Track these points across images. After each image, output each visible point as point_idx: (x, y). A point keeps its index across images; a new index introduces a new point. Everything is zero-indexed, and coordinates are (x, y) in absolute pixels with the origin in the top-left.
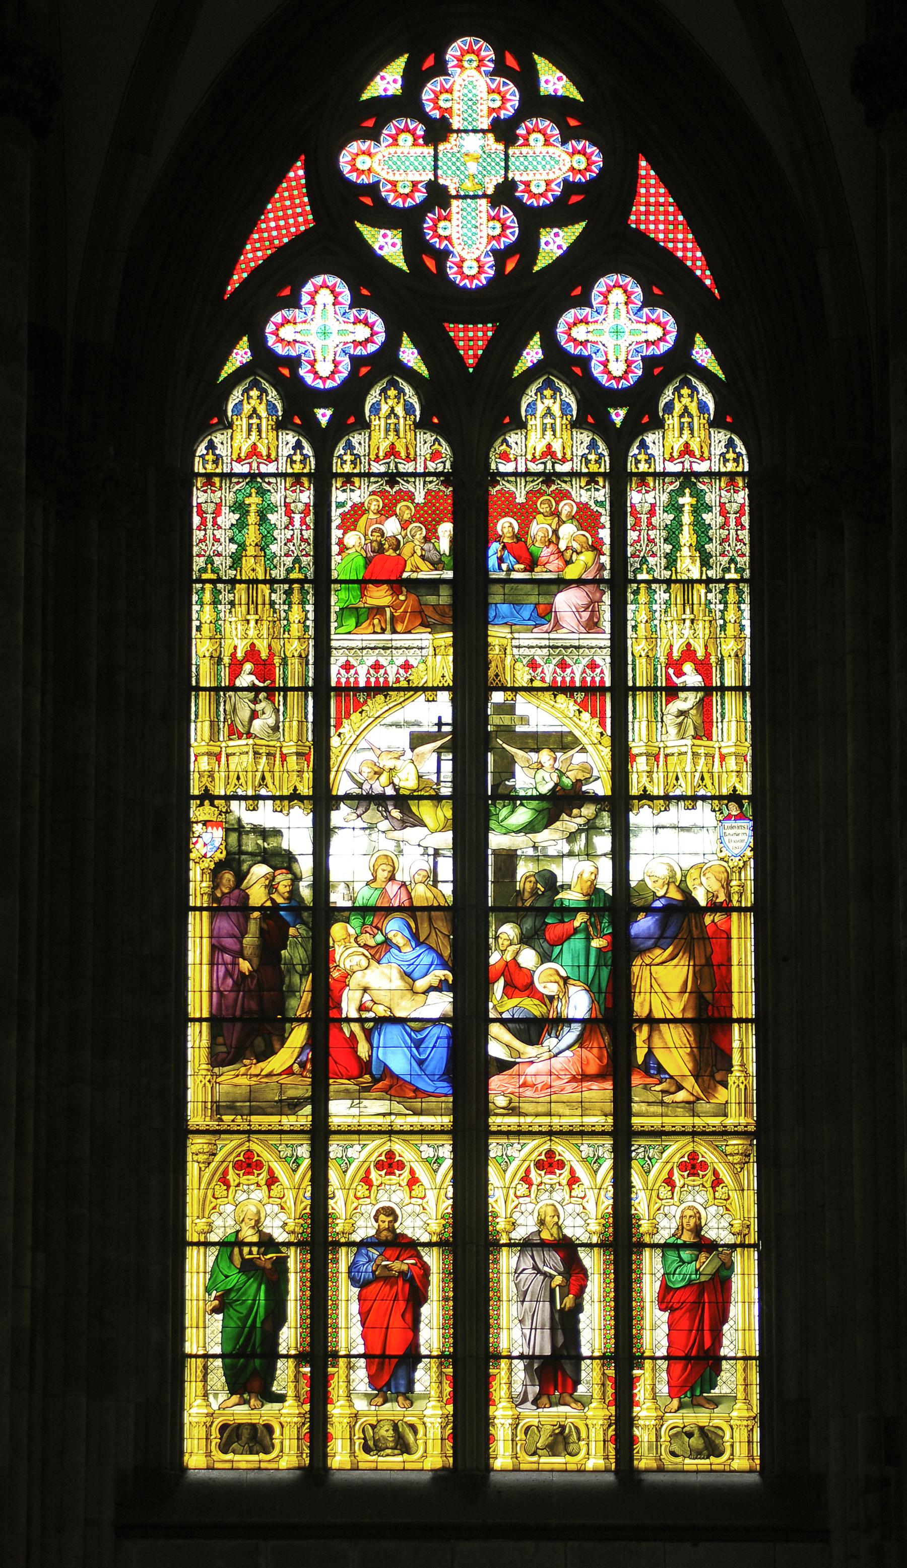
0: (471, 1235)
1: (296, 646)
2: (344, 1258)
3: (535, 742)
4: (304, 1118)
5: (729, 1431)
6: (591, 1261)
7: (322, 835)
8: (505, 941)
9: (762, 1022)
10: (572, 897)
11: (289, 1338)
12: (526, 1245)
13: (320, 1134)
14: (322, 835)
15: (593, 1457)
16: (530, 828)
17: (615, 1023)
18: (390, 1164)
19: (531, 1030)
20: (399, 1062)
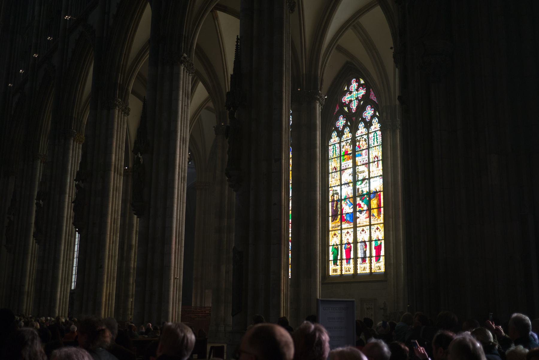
0: (355, 242)
1: (338, 165)
2: (344, 246)
3: (361, 172)
4: (339, 228)
5: (379, 266)
6: (368, 243)
7: (341, 189)
8: (358, 201)
9: (384, 207)
10: (365, 193)
11: (339, 257)
12: (361, 242)
13: (341, 229)
14: (341, 189)
15: (368, 271)
16: (360, 184)
17: (369, 209)
18: (348, 233)
19: (361, 212)
20: (348, 219)
